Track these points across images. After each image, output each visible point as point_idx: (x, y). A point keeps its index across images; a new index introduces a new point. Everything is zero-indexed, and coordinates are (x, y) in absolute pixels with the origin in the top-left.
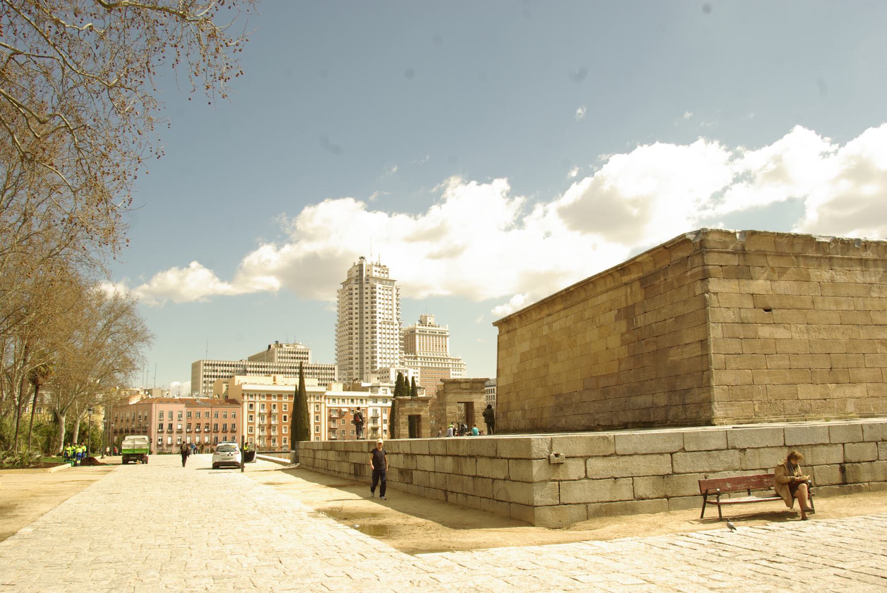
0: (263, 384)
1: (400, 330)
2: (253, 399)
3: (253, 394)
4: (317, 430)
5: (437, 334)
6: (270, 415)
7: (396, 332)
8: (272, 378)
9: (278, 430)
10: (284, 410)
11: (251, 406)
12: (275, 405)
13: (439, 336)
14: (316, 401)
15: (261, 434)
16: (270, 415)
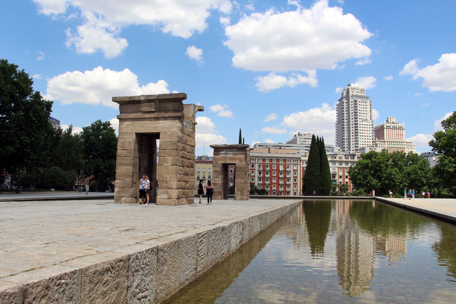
0: (262, 153)
1: (372, 125)
2: (254, 162)
3: (254, 158)
4: (295, 180)
5: (391, 127)
6: (264, 170)
7: (370, 126)
8: (268, 149)
9: (270, 181)
10: (273, 169)
11: (253, 166)
12: (268, 165)
13: (393, 129)
14: (295, 163)
15: (260, 182)
16: (264, 170)
